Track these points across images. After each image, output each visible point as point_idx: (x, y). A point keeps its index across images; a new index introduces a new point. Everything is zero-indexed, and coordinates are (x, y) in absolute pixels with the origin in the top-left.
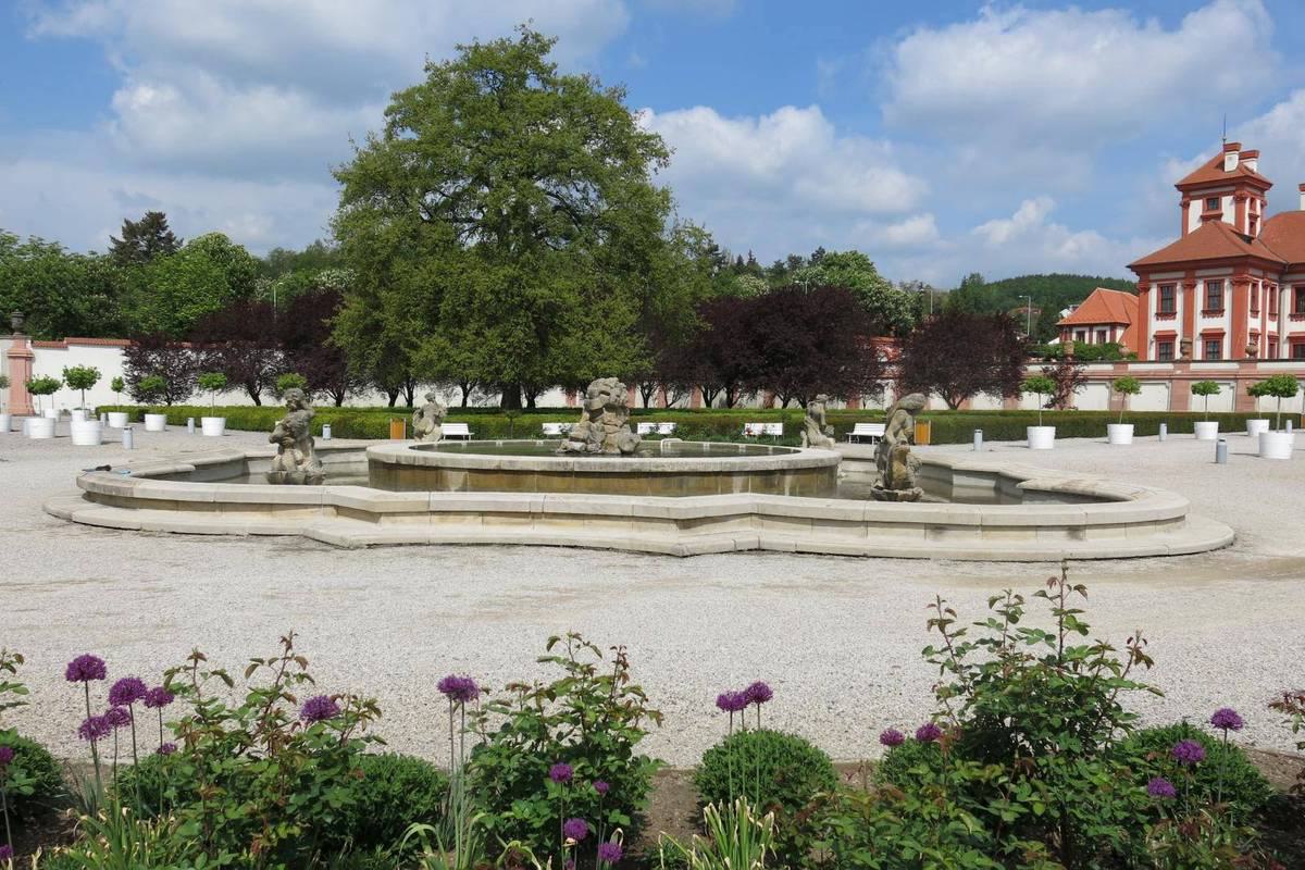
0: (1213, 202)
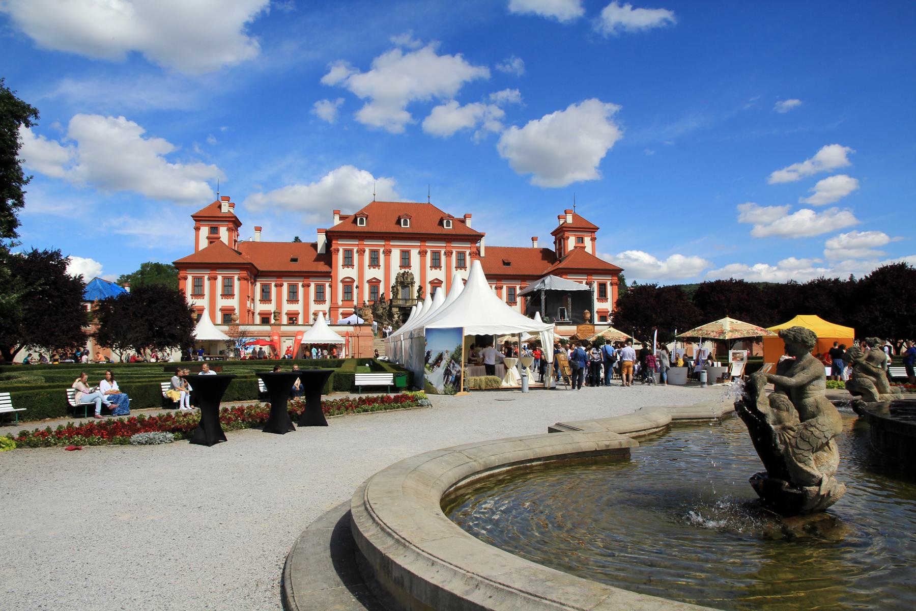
0: (214, 230)
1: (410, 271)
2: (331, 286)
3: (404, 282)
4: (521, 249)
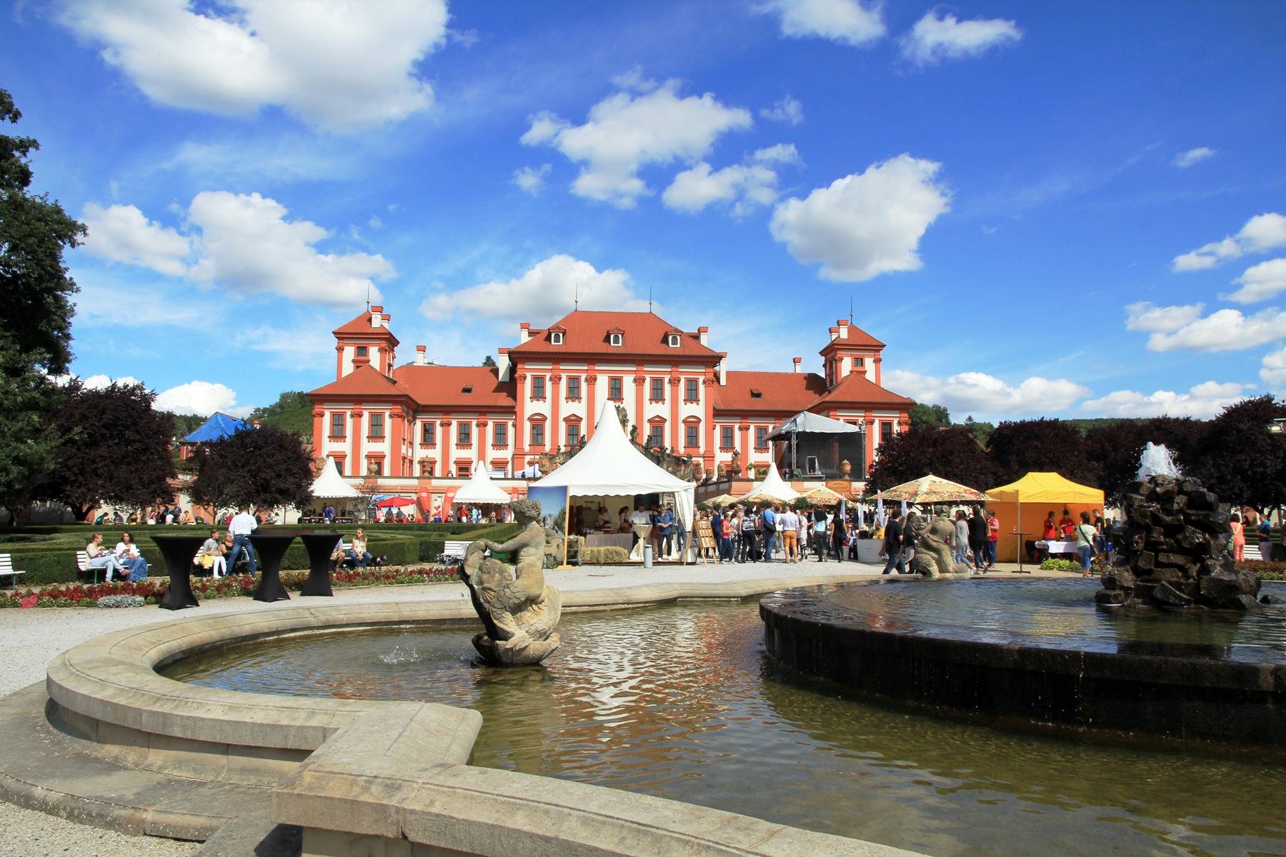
0: (362, 350)
1: (622, 406)
2: (514, 425)
4: (777, 374)
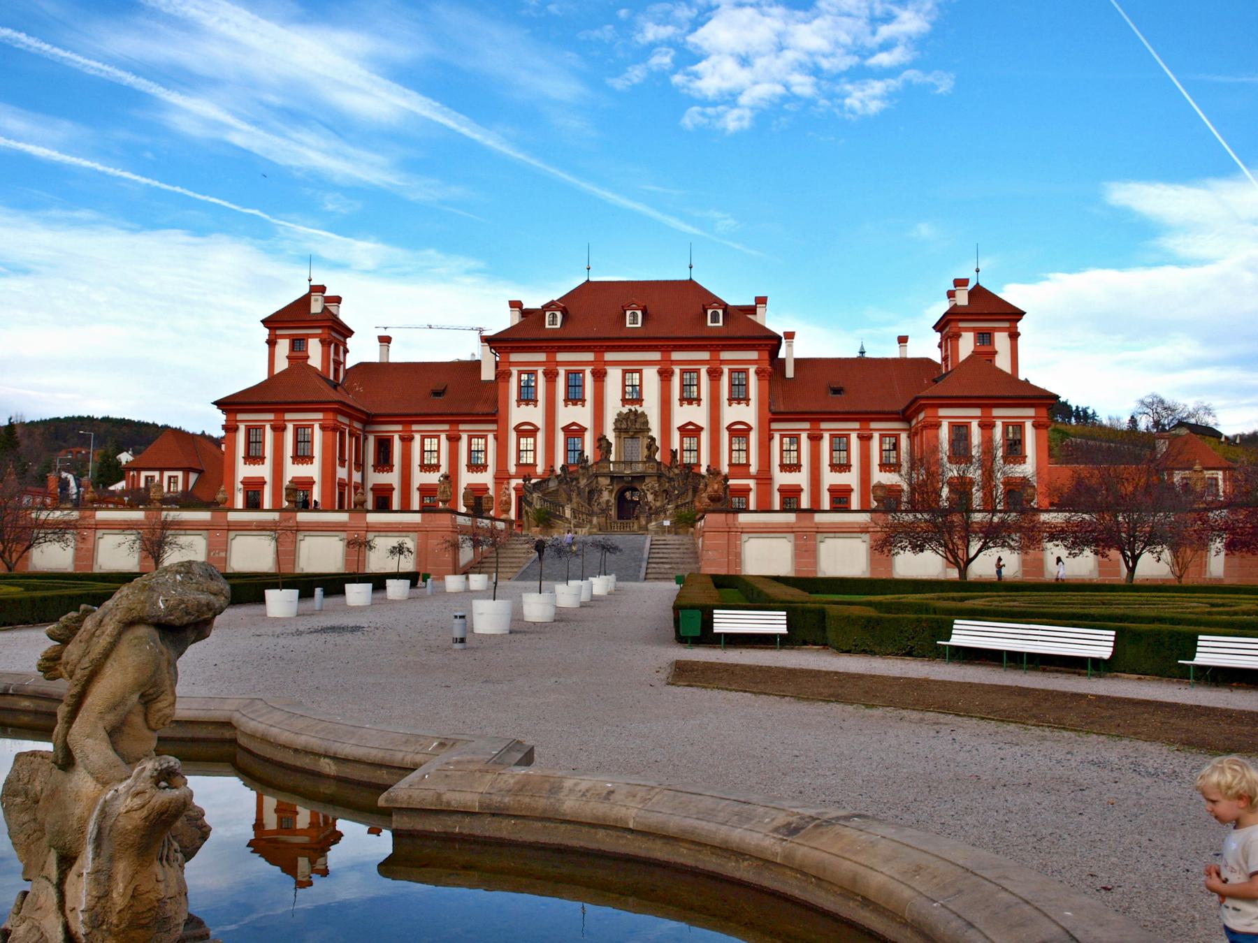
1: (640, 410)
2: (496, 438)
3: (632, 425)
